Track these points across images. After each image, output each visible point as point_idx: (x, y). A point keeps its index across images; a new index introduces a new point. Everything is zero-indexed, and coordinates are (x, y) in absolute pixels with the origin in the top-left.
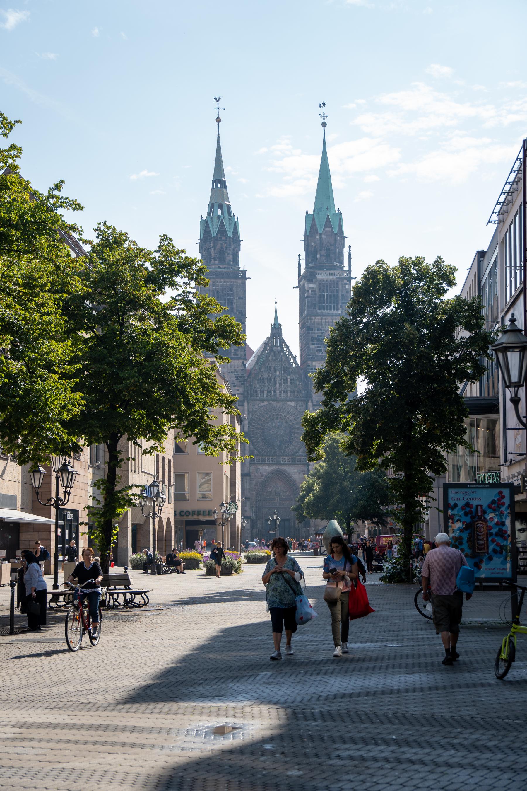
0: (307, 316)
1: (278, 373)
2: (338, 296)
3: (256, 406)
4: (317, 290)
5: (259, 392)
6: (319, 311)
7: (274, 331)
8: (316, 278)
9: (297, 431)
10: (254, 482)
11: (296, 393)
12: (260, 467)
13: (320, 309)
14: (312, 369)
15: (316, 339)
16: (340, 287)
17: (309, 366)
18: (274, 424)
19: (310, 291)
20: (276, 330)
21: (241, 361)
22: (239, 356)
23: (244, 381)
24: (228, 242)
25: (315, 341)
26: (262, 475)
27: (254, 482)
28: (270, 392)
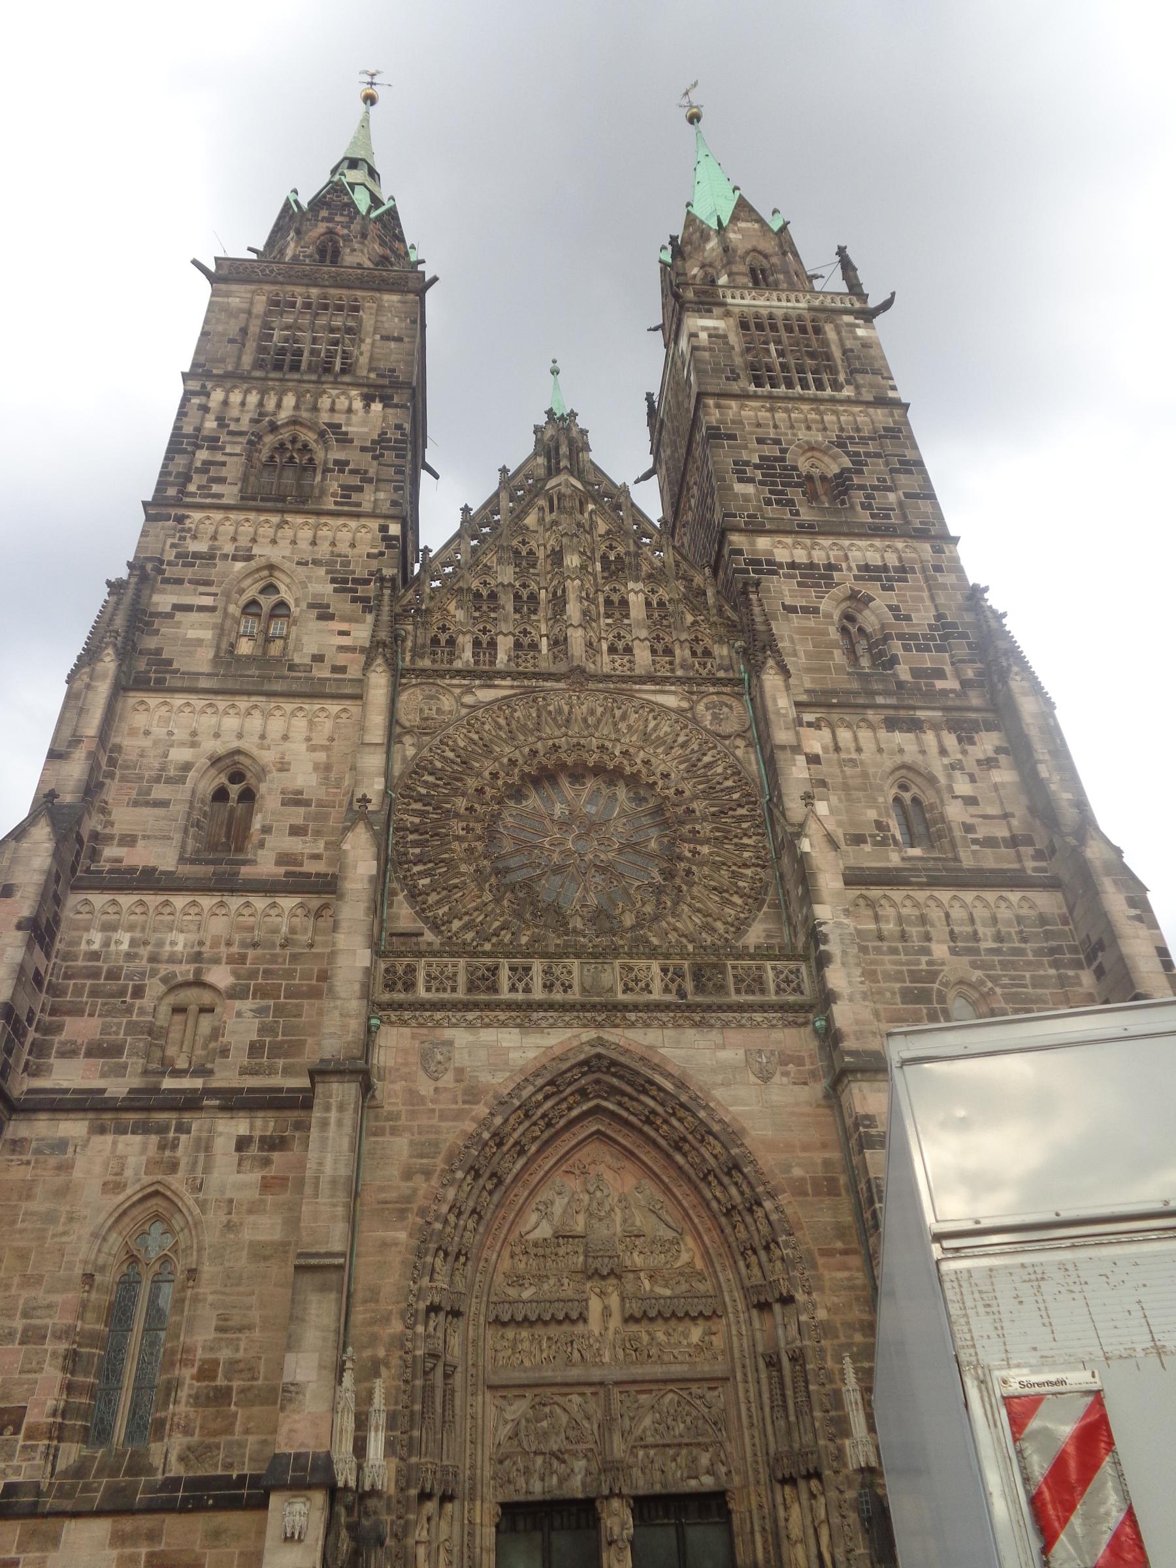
0: (700, 396)
1: (572, 561)
2: (828, 356)
3: (447, 703)
4: (733, 339)
5: (465, 642)
6: (752, 388)
7: (550, 432)
8: (724, 304)
9: (705, 829)
10: (400, 1147)
11: (681, 653)
12: (461, 1037)
13: (759, 385)
14: (755, 562)
15: (757, 467)
16: (831, 335)
17: (739, 552)
18: (559, 809)
19: (704, 336)
20: (561, 443)
21: (374, 524)
22: (367, 507)
23: (379, 597)
24: (356, 227)
25: (758, 475)
26: (473, 1094)
27: (400, 1147)
28: (534, 646)
